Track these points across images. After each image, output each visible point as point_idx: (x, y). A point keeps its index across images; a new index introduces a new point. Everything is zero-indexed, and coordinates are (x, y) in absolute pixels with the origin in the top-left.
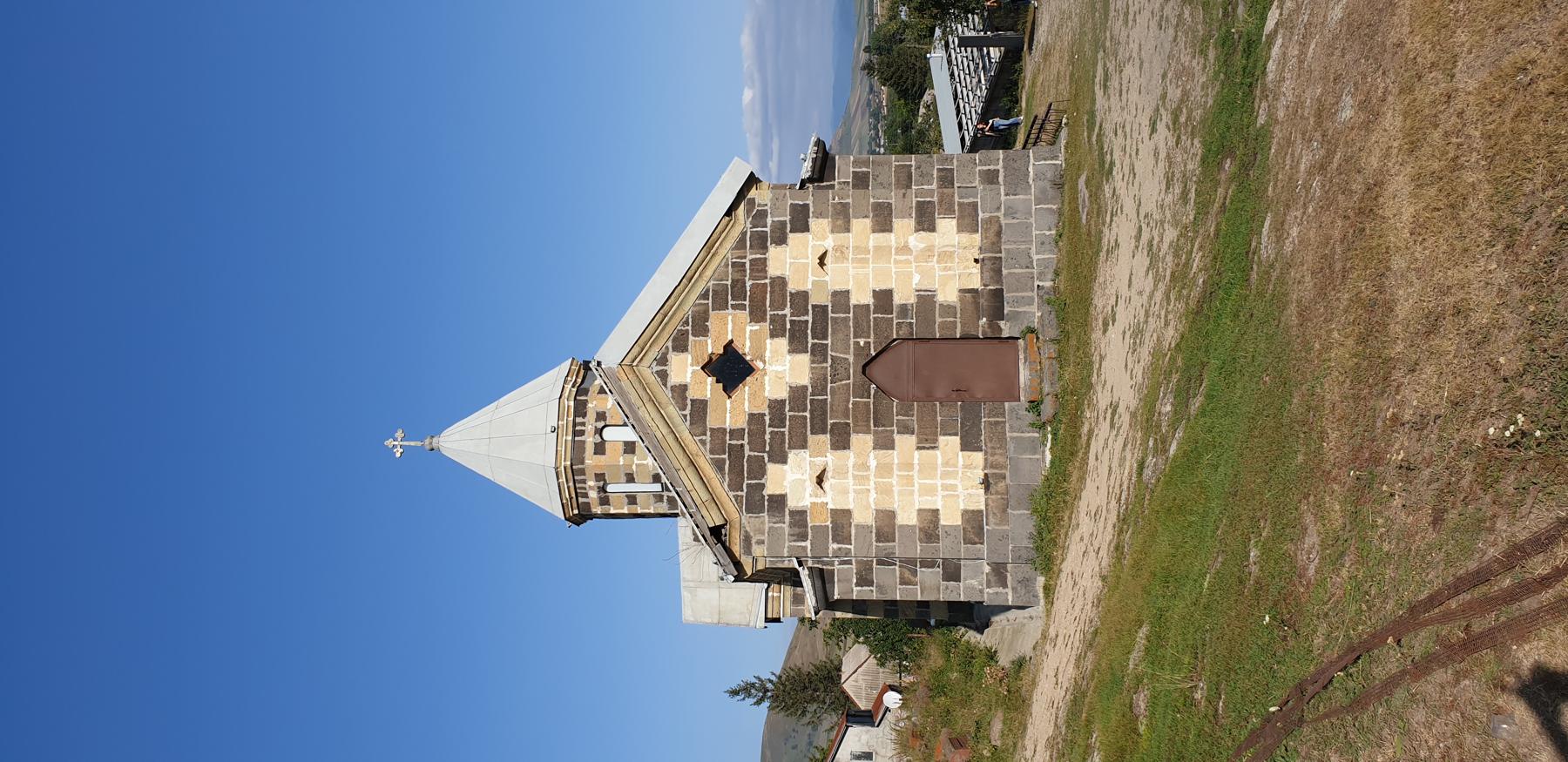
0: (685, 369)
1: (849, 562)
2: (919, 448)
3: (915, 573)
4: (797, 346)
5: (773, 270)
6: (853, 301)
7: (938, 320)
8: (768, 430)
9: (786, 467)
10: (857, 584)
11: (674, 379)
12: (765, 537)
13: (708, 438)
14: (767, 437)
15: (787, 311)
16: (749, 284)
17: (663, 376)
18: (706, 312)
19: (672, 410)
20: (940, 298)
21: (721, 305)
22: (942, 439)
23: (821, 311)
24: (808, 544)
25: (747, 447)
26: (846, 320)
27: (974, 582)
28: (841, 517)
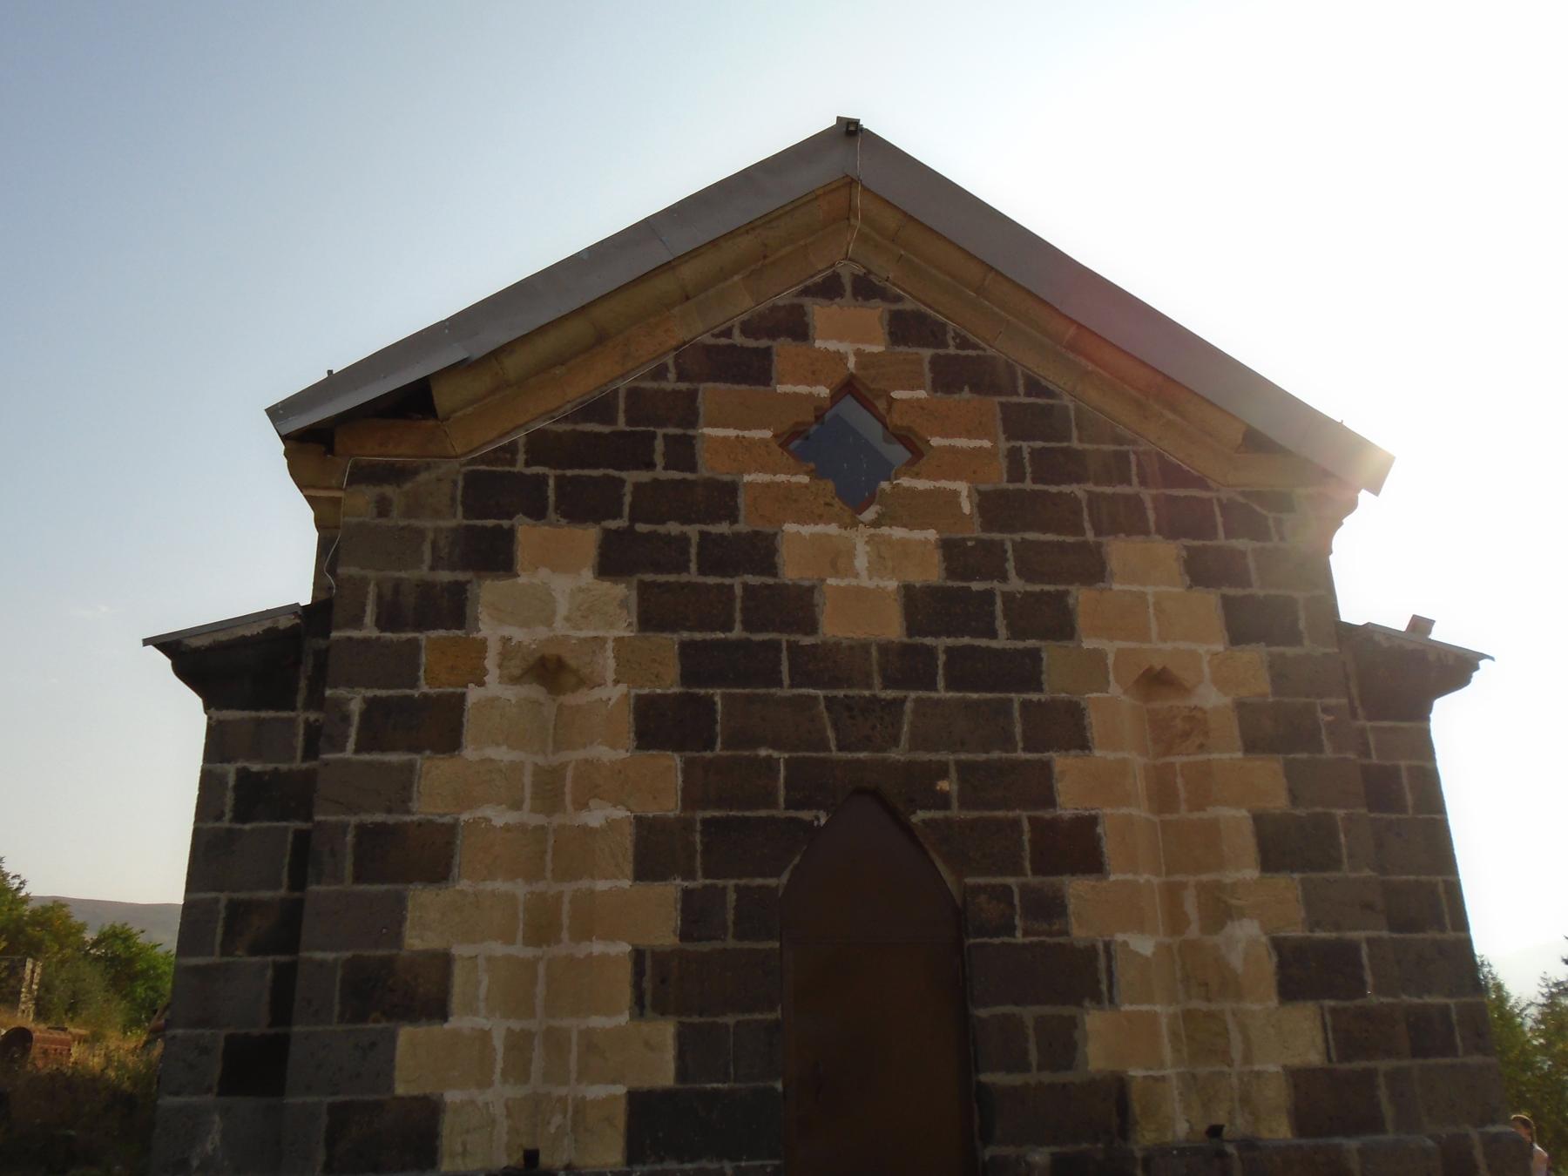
0: (846, 337)
1: (311, 751)
2: (638, 955)
4: (922, 607)
5: (1120, 551)
6: (1061, 762)
7: (1029, 1014)
8: (693, 531)
9: (587, 576)
10: (243, 775)
11: (819, 313)
12: (396, 520)
13: (671, 384)
14: (674, 528)
15: (1016, 584)
16: (1078, 490)
17: (829, 289)
18: (994, 389)
19: (742, 304)
20: (1094, 1021)
21: (1017, 423)
22: (665, 1031)
23: (1026, 671)
24: (369, 631)
25: (644, 476)
26: (1007, 742)
28: (441, 725)
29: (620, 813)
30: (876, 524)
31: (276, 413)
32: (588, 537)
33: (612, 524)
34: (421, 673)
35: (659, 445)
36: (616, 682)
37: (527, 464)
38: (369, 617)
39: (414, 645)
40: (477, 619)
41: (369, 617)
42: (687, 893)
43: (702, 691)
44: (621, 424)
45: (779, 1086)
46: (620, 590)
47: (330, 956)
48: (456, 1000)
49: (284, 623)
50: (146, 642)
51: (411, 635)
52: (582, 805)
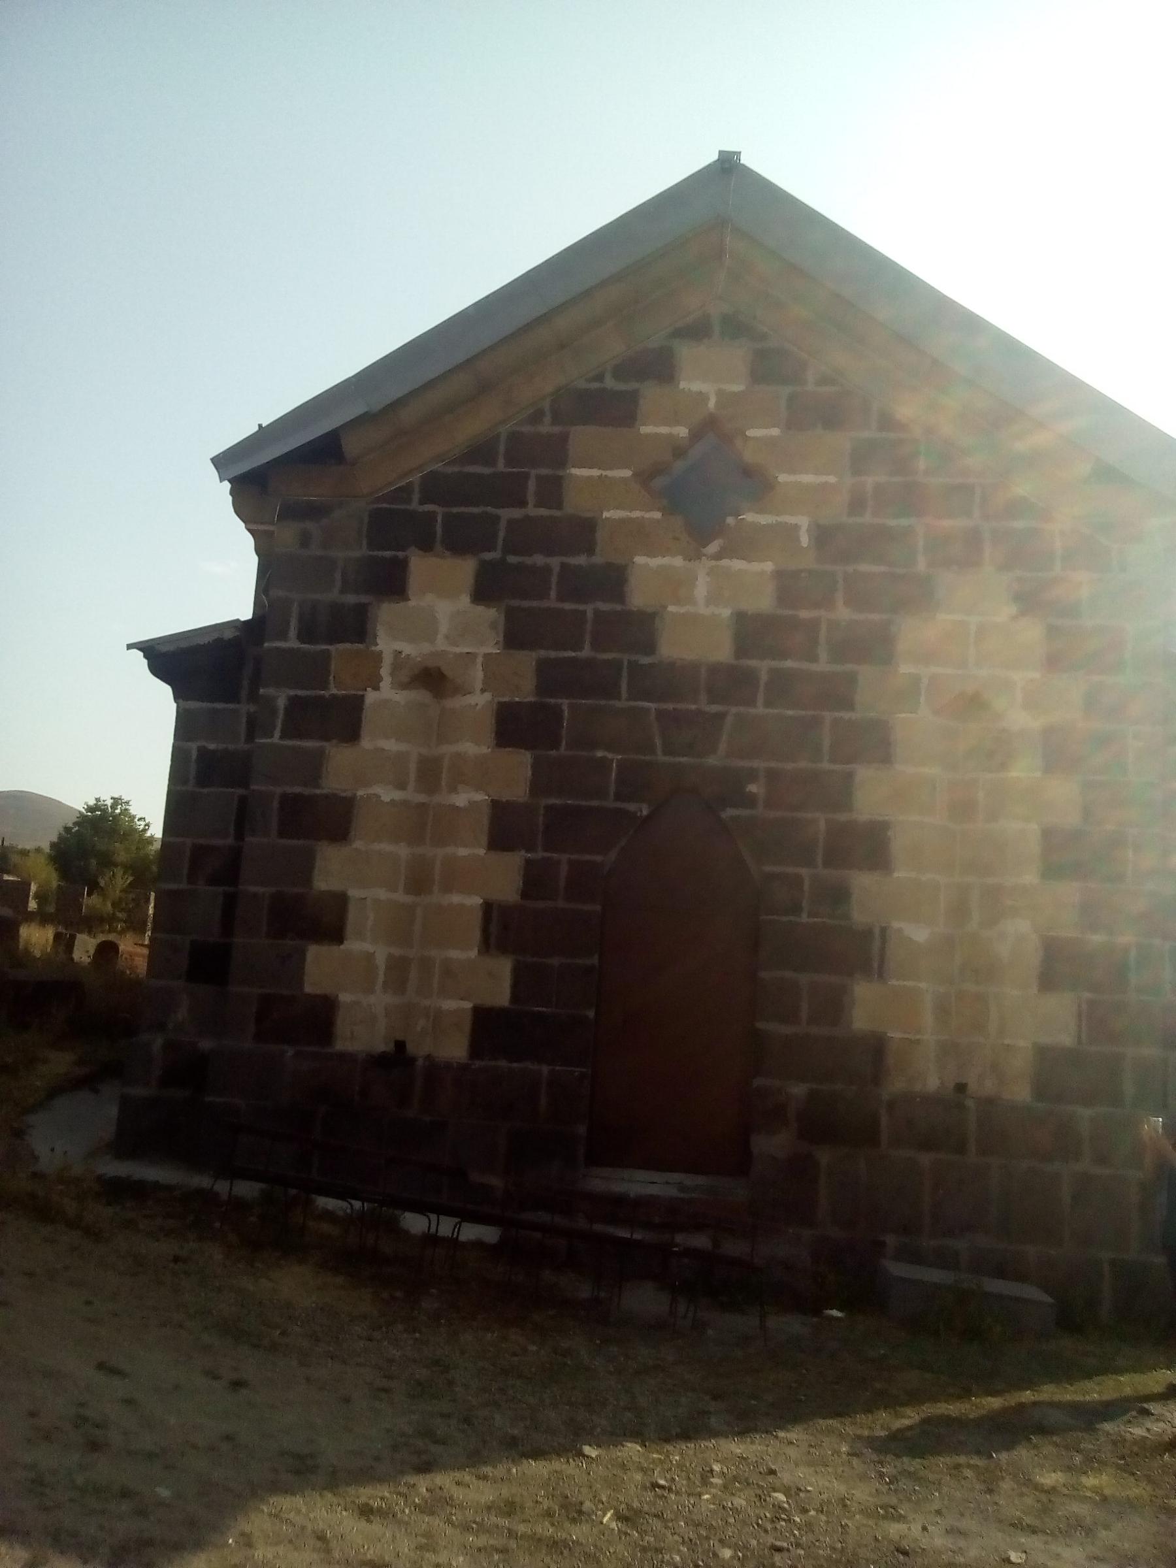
1: (250, 737)
2: (488, 907)
3: (213, 881)
9: (465, 600)
13: (546, 428)
14: (539, 560)
22: (504, 967)
24: (292, 643)
25: (516, 513)
27: (182, 1014)
28: (345, 719)
29: (480, 797)
30: (718, 556)
31: (221, 462)
32: (465, 569)
33: (488, 556)
34: (331, 678)
35: (532, 485)
36: (483, 691)
37: (421, 503)
38: (293, 633)
39: (327, 655)
40: (375, 636)
42: (528, 862)
43: (553, 701)
44: (501, 466)
45: (591, 1014)
46: (490, 614)
47: (260, 890)
48: (350, 929)
49: (228, 635)
50: (129, 647)
51: (324, 647)
52: (453, 789)
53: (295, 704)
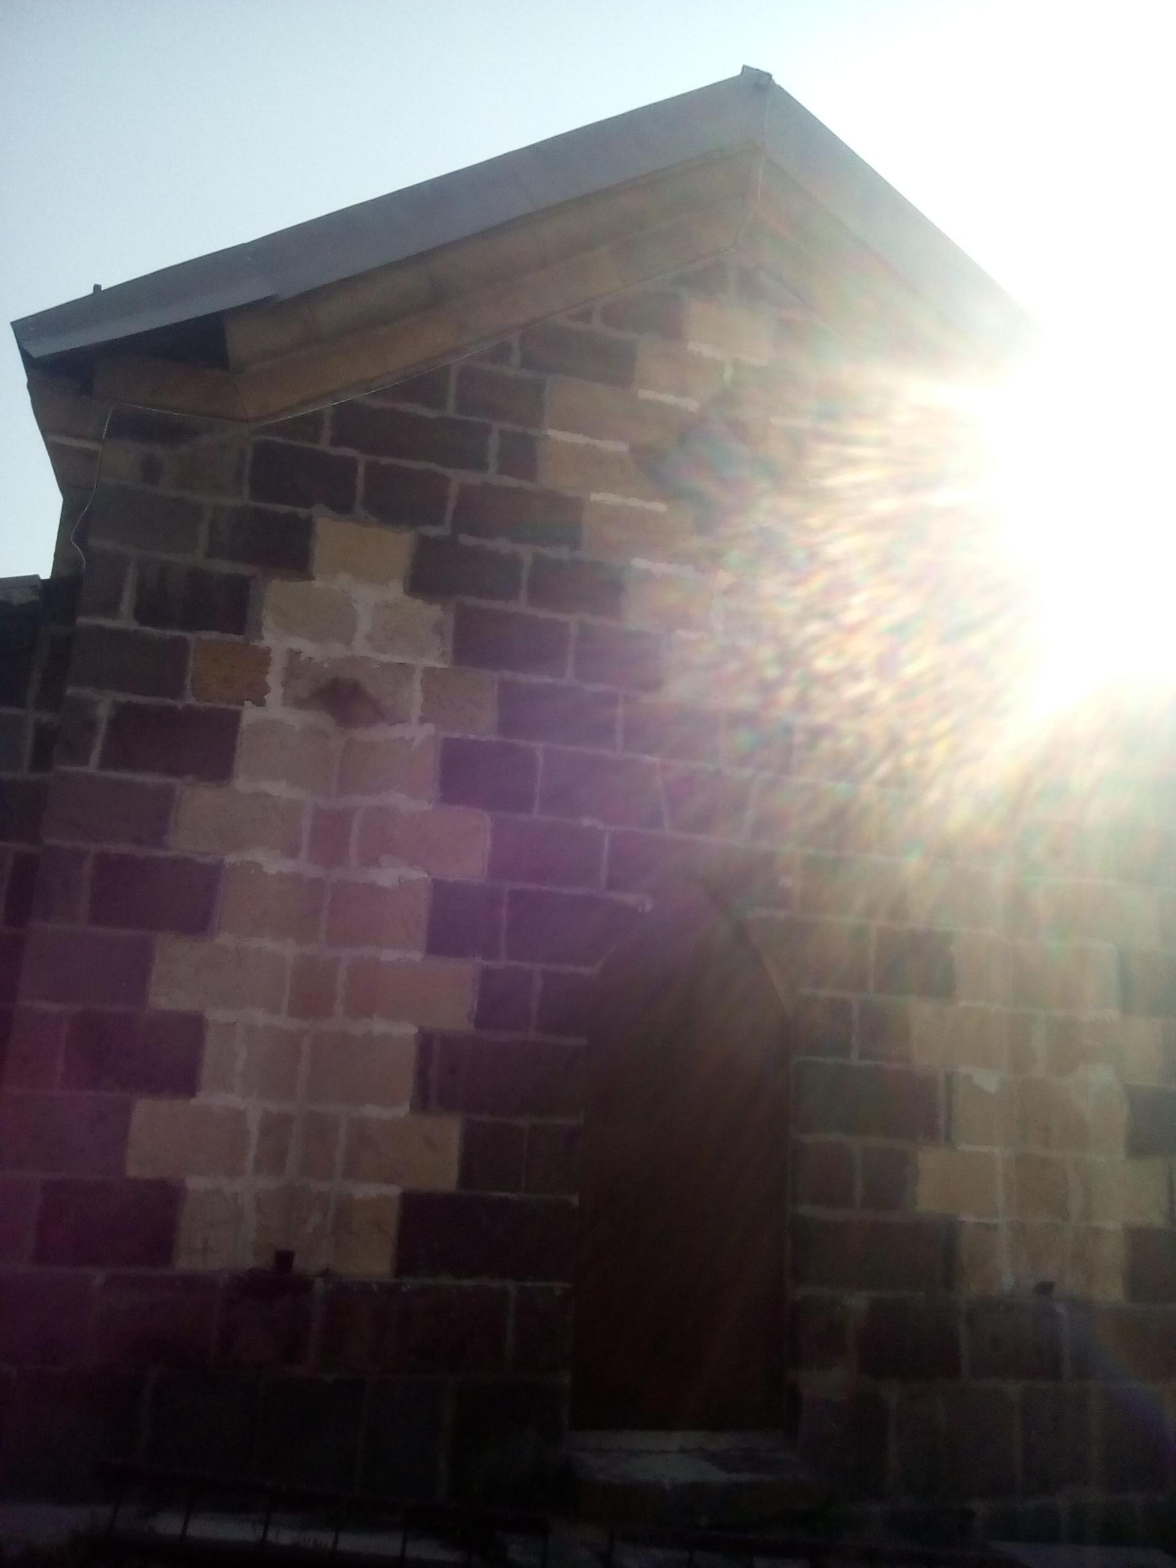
1: (42, 758)
9: (395, 590)
24: (125, 620)
28: (208, 745)
29: (417, 875)
31: (26, 330)
33: (432, 531)
34: (188, 681)
35: (494, 443)
36: (423, 720)
37: (335, 442)
38: (126, 606)
39: (180, 647)
40: (259, 625)
41: (126, 606)
42: (487, 975)
45: (575, 1200)
46: (433, 612)
48: (206, 1073)
49: (19, 598)
51: (176, 633)
52: (371, 860)
53: (124, 717)
